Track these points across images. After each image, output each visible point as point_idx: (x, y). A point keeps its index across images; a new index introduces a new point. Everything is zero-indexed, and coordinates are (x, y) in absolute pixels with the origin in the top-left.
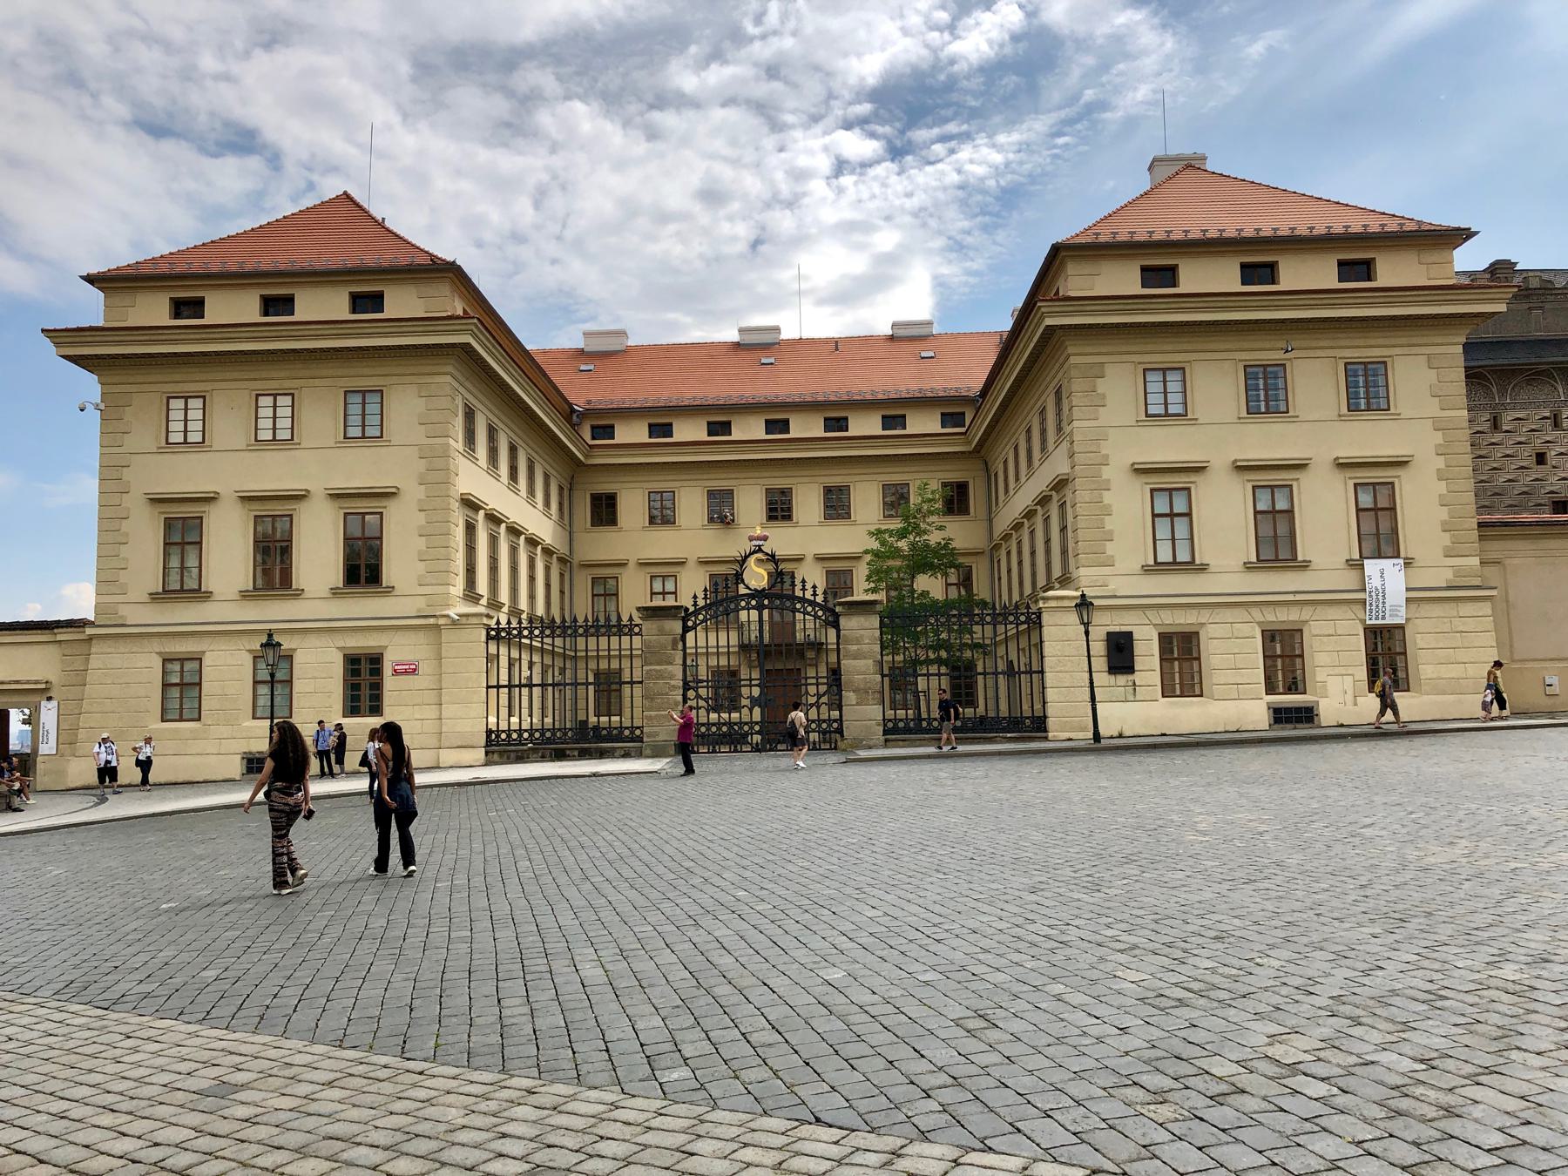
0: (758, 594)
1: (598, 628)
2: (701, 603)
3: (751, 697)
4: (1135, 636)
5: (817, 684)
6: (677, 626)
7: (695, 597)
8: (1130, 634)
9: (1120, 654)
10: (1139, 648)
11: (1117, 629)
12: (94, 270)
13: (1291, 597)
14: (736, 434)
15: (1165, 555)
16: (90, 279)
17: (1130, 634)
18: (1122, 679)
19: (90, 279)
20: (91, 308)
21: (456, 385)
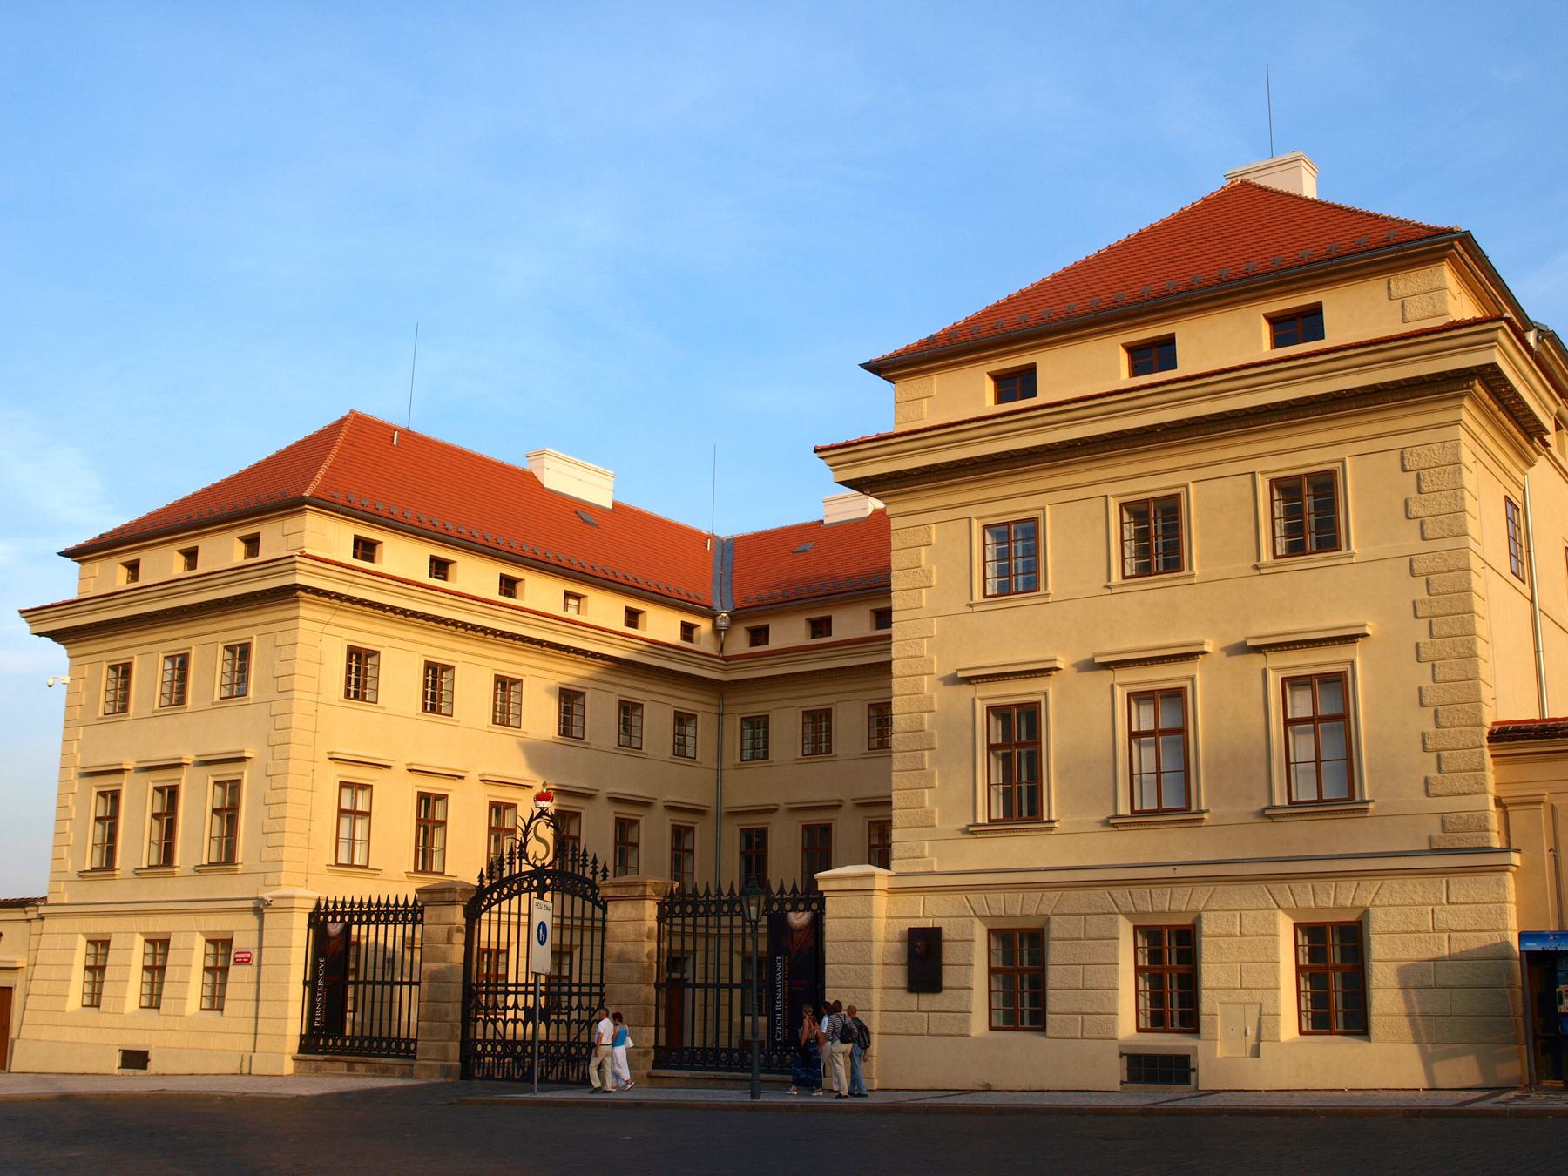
0: (539, 872)
1: (719, 904)
2: (487, 883)
3: (526, 1008)
4: (945, 934)
5: (590, 994)
6: (458, 915)
7: (481, 875)
8: (939, 929)
9: (923, 958)
10: (949, 954)
11: (928, 923)
12: (71, 545)
13: (1182, 872)
14: (775, 643)
15: (1306, 792)
16: (66, 554)
17: (939, 929)
18: (927, 1001)
19: (66, 554)
20: (64, 583)
21: (319, 627)
